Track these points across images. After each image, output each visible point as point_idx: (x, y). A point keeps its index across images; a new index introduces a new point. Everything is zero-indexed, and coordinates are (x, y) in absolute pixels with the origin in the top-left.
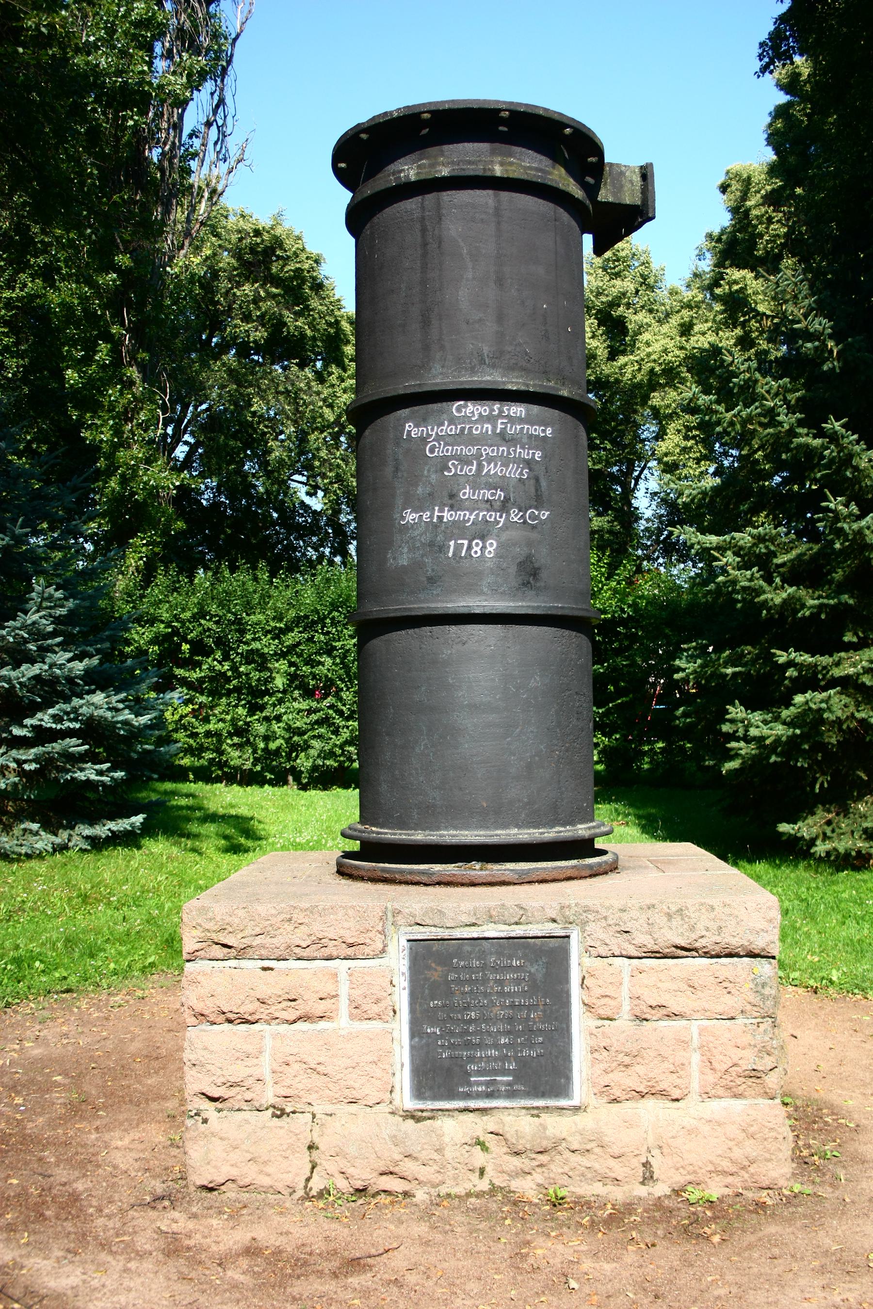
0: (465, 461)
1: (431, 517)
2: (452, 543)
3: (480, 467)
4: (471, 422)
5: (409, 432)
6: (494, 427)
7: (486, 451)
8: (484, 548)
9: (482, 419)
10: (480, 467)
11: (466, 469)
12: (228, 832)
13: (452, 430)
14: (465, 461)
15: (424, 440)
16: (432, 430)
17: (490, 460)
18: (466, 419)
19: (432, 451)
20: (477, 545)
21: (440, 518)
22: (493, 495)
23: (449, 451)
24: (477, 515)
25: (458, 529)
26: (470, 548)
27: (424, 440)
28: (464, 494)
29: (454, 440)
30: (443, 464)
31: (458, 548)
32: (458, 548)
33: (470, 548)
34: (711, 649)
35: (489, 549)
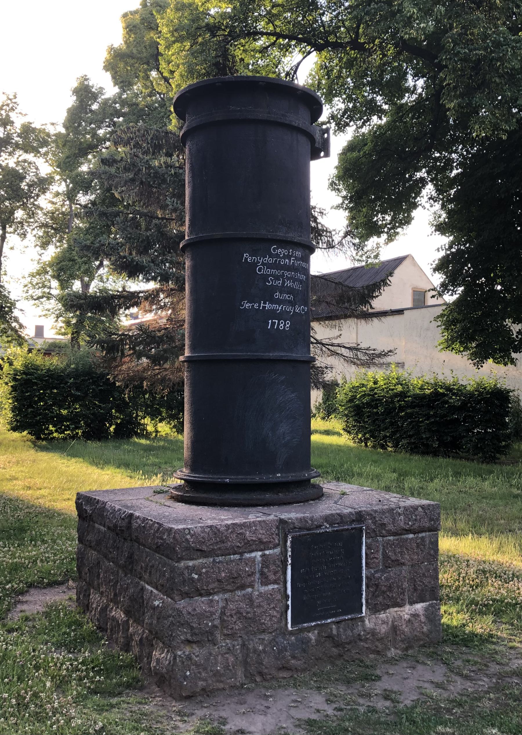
0: (277, 278)
1: (259, 306)
2: (270, 321)
3: (284, 282)
4: (280, 258)
5: (246, 259)
6: (290, 261)
7: (287, 274)
8: (285, 325)
9: (285, 257)
10: (284, 282)
11: (277, 282)
12: (30, 492)
13: (271, 261)
14: (277, 278)
15: (255, 265)
16: (260, 259)
17: (288, 279)
18: (277, 256)
19: (260, 270)
20: (282, 323)
21: (264, 307)
22: (289, 297)
23: (269, 271)
24: (282, 307)
25: (273, 315)
26: (279, 324)
27: (255, 265)
28: (276, 296)
29: (269, 266)
30: (265, 278)
31: (273, 324)
32: (273, 324)
33: (279, 324)
34: (466, 268)
35: (288, 326)
